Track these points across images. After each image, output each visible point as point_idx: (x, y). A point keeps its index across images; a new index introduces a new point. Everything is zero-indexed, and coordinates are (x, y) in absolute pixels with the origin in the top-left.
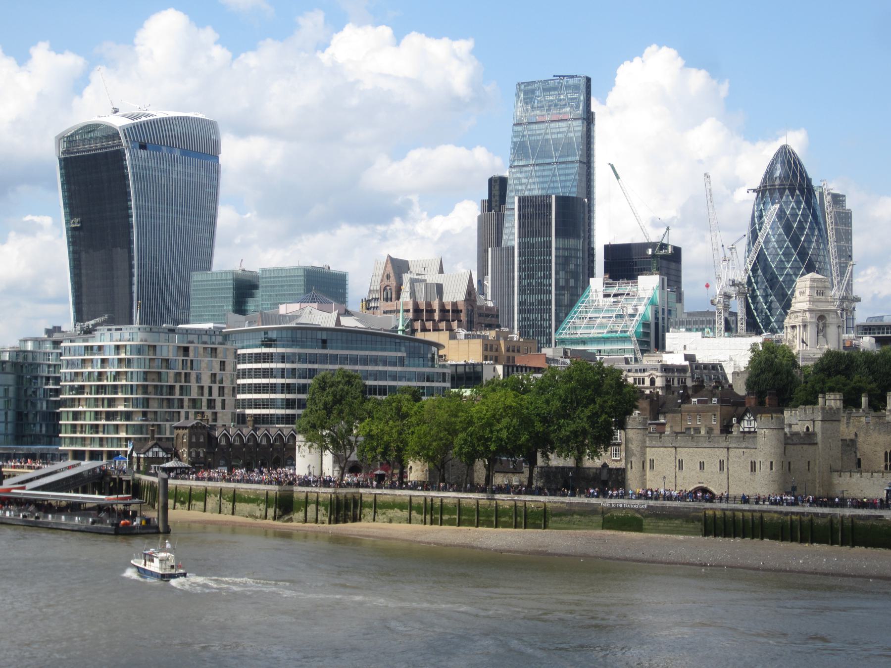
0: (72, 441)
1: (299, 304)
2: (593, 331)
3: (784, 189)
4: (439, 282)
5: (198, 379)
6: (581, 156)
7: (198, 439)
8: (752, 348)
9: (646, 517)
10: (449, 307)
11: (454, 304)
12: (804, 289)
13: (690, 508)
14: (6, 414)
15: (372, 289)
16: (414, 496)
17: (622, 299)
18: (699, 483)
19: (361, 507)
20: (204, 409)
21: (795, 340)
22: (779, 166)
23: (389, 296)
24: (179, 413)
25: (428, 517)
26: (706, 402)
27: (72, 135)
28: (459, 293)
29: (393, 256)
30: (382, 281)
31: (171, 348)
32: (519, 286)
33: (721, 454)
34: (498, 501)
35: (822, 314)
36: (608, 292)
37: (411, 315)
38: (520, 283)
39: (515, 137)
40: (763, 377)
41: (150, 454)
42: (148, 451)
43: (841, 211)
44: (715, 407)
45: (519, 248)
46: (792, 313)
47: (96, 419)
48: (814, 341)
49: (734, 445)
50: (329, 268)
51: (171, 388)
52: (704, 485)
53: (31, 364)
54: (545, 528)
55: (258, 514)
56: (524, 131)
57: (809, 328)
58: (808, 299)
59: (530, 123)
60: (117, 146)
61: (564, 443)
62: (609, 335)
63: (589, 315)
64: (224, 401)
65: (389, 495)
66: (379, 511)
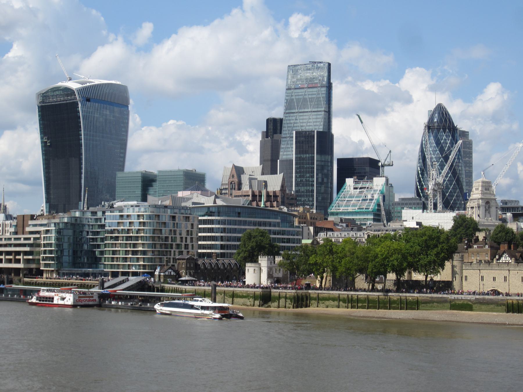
0: (112, 266)
1: (190, 191)
2: (349, 208)
3: (440, 129)
5: (180, 234)
6: (325, 108)
7: (190, 265)
8: (454, 219)
9: (475, 304)
10: (272, 194)
11: (274, 192)
12: (478, 187)
13: (499, 299)
14: (69, 251)
15: (223, 183)
16: (341, 294)
17: (365, 190)
18: (493, 287)
19: (310, 300)
20: (183, 249)
21: (473, 215)
22: (436, 115)
23: (234, 187)
24: (170, 251)
25: (350, 305)
26: (482, 247)
27: (45, 93)
28: (277, 186)
29: (236, 165)
30: (229, 178)
31: (167, 216)
32: (295, 182)
33: (506, 273)
34: (390, 296)
35: (488, 201)
36: (356, 186)
37: (250, 198)
38: (296, 180)
39: (287, 96)
40: (500, 235)
41: (167, 273)
42: (166, 271)
43: (467, 140)
44: (488, 250)
45: (296, 160)
46: (471, 200)
47: (126, 255)
48: (484, 215)
49: (512, 269)
50: (195, 170)
51: (167, 238)
52: (496, 289)
53: (79, 224)
54: (417, 310)
55: (249, 303)
56: (292, 93)
57: (481, 208)
58: (480, 192)
59: (295, 89)
60: (74, 99)
61: (423, 267)
62: (359, 210)
63: (346, 199)
64: (193, 245)
65: (326, 293)
66: (320, 302)
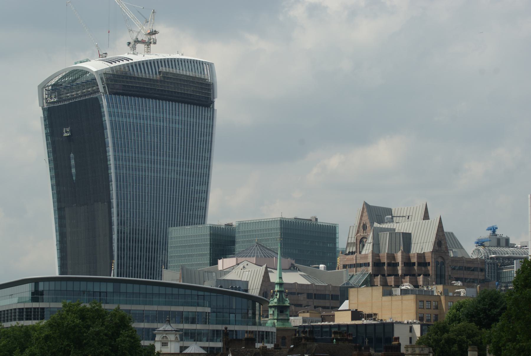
4: (405, 232)
11: (421, 256)
15: (349, 241)
28: (427, 243)
29: (371, 204)
37: (370, 269)
50: (316, 219)
